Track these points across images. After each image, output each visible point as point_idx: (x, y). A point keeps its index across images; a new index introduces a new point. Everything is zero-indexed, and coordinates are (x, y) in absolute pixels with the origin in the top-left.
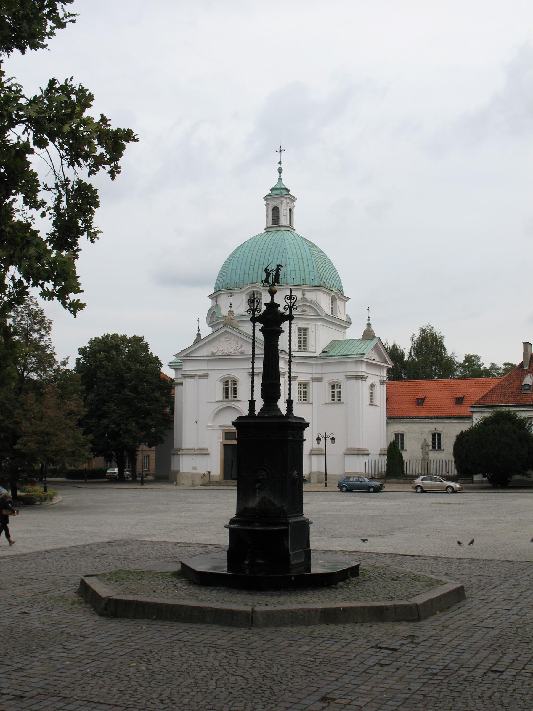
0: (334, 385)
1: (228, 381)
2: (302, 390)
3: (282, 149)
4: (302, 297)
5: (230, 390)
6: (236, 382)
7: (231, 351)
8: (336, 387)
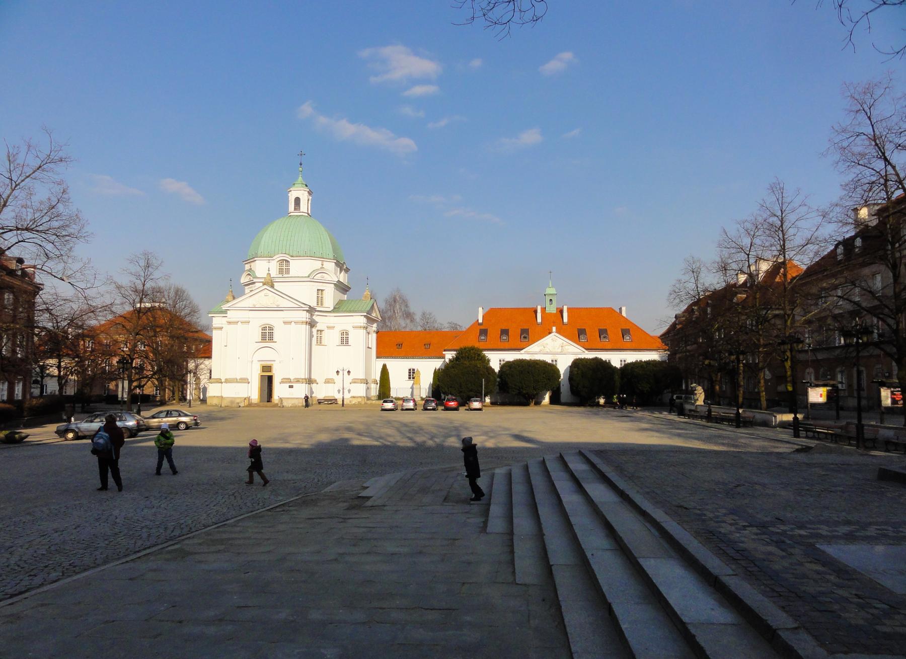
1: (266, 327)
2: (319, 335)
4: (321, 266)
5: (267, 334)
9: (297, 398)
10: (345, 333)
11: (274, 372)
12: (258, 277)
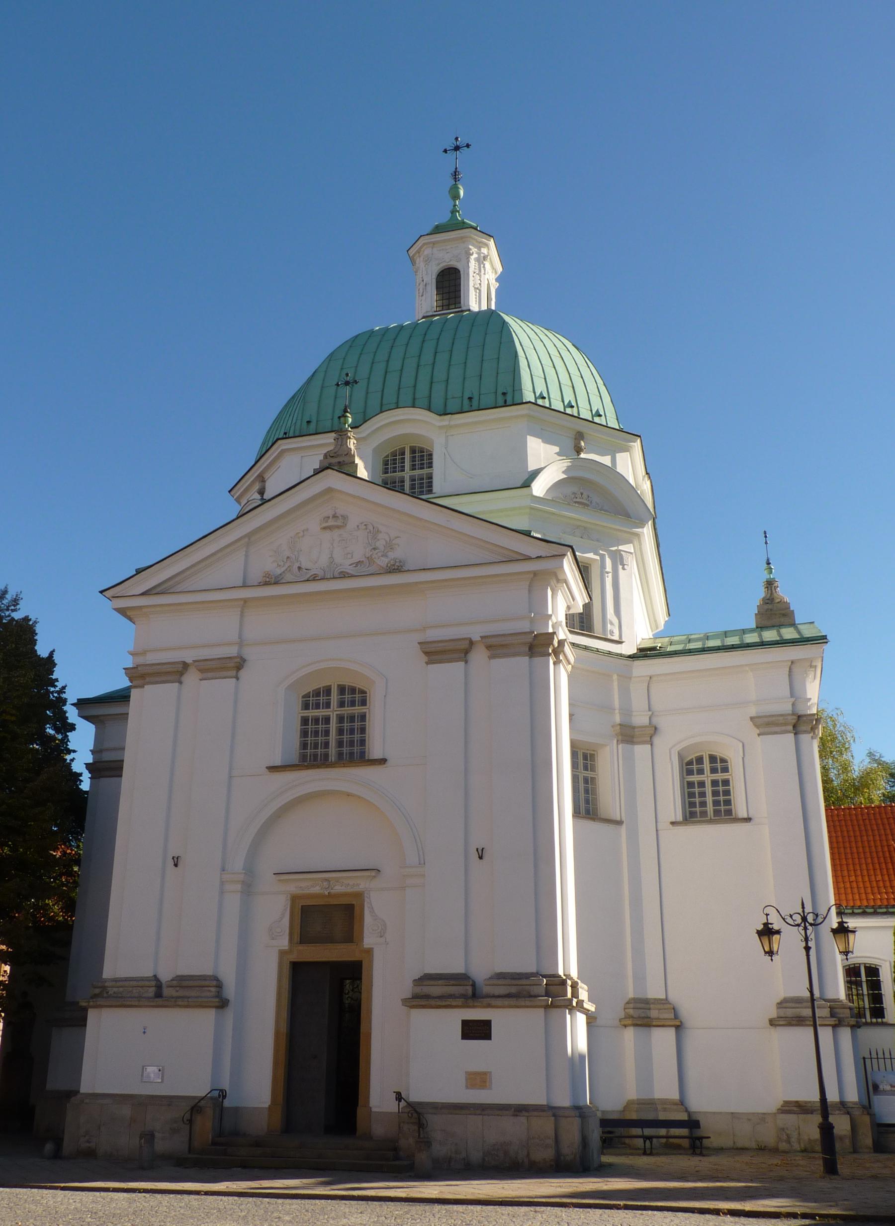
0: (700, 760)
5: (333, 726)
6: (363, 692)
8: (707, 765)
9: (520, 1110)
10: (706, 761)
11: (369, 940)
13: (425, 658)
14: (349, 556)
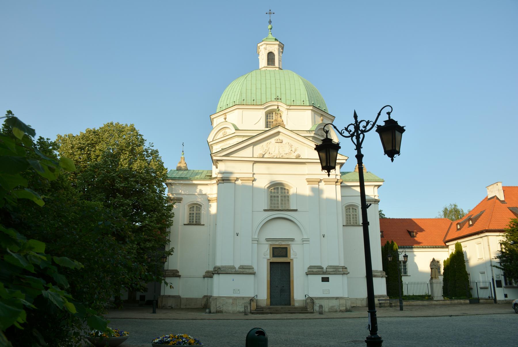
3: (272, 11)
5: (280, 199)
6: (287, 190)
7: (283, 155)
9: (337, 298)
11: (292, 257)
12: (240, 129)
13: (307, 183)
14: (284, 151)
